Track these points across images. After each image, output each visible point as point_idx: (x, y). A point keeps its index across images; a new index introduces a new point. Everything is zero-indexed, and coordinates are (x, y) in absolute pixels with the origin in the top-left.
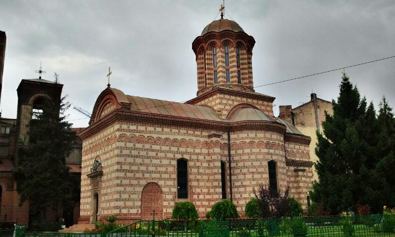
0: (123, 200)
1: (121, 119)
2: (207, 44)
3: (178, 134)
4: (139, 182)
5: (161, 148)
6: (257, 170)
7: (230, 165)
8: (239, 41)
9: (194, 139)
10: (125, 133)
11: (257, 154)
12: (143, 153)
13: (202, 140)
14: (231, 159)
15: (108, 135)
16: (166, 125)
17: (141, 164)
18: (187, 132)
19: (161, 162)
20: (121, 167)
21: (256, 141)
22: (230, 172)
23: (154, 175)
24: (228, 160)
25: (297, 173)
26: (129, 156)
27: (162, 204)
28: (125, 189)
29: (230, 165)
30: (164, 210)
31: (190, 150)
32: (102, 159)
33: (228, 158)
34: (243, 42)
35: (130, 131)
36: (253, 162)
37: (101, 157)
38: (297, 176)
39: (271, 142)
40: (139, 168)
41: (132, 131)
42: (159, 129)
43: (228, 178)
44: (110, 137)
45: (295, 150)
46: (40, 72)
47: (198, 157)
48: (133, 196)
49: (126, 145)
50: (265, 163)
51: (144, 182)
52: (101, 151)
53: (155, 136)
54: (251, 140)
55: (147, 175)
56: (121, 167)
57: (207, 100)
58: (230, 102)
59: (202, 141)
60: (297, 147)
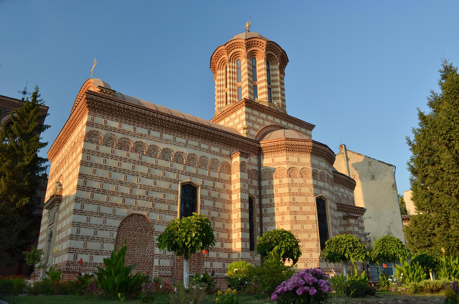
0: (82, 238)
1: (94, 107)
2: (230, 55)
3: (186, 145)
4: (114, 211)
5: (156, 162)
6: (301, 208)
7: (260, 202)
8: (269, 54)
9: (210, 156)
10: (96, 130)
11: (301, 185)
12: (126, 166)
13: (221, 159)
14: (263, 194)
15: (75, 138)
16: (167, 129)
17: (121, 183)
18: (200, 145)
19: (155, 183)
20: (85, 182)
21: (300, 167)
22: (261, 211)
23: (141, 203)
24: (258, 194)
25: (348, 222)
26: (101, 167)
27: (153, 251)
28: (88, 220)
29: (260, 202)
30: (156, 262)
31: (202, 172)
32: (64, 178)
33: (258, 191)
34: (275, 56)
35: (106, 128)
36: (296, 197)
37: (64, 175)
38: (348, 225)
39: (320, 171)
40: (117, 188)
41: (111, 129)
42: (155, 134)
43: (257, 219)
44: (76, 140)
45: (340, 194)
46: (25, 93)
47: (214, 184)
48: (100, 234)
49: (97, 148)
50: (312, 200)
51: (124, 212)
52: (65, 167)
53: (148, 143)
54: (292, 166)
55: (129, 201)
56: (85, 182)
57: (227, 119)
58: (261, 121)
59: (221, 162)
60: (342, 190)
